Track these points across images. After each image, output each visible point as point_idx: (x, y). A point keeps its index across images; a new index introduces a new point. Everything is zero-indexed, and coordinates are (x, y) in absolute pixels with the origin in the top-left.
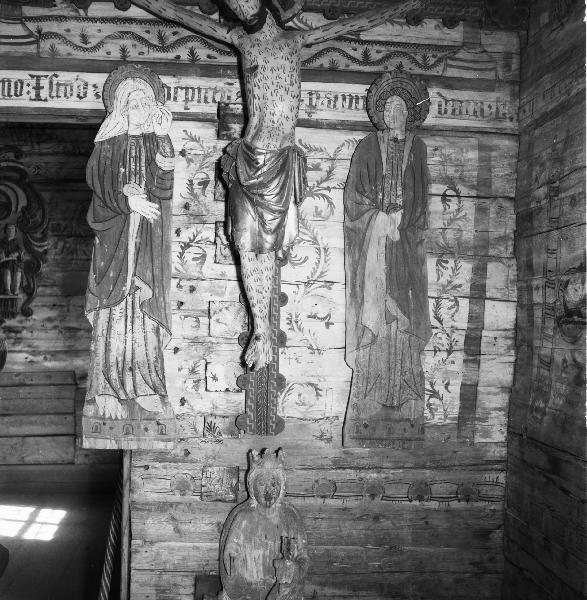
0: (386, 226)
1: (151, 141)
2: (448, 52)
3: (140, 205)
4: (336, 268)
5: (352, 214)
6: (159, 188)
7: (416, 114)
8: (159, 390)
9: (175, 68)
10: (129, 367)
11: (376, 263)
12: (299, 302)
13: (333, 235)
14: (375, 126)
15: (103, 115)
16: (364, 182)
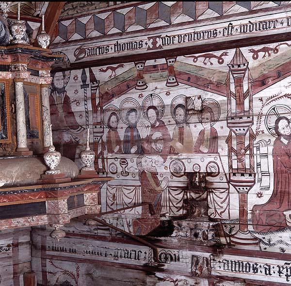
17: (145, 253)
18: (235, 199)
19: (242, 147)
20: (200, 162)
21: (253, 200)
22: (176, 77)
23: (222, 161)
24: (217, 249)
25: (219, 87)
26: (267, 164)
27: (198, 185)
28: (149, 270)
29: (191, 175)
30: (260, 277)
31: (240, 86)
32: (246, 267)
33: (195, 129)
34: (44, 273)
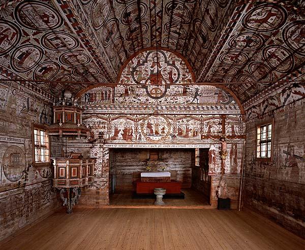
0: (234, 157)
1: (214, 150)
2: (239, 141)
3: (213, 156)
4: (229, 160)
5: (231, 156)
6: (214, 154)
7: (236, 147)
8: (215, 170)
9: (215, 144)
10: (212, 169)
11: (233, 159)
12: (226, 163)
13: (229, 158)
14: (232, 148)
15: (209, 148)
16: (231, 153)
17: (91, 145)
18: (108, 136)
19: (109, 128)
20: (102, 130)
21: (111, 136)
22: (99, 117)
23: (106, 130)
24: (104, 143)
25: (106, 120)
26: (114, 131)
27: (101, 134)
28: (91, 148)
29: (100, 132)
30: (112, 147)
31: (109, 120)
32: (109, 146)
33: (101, 126)
34: (66, 151)
